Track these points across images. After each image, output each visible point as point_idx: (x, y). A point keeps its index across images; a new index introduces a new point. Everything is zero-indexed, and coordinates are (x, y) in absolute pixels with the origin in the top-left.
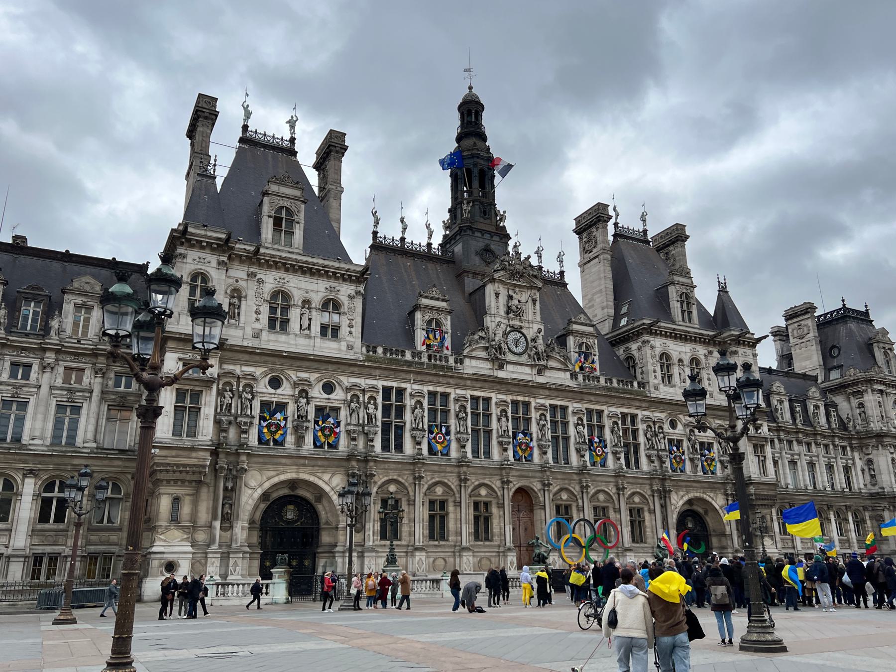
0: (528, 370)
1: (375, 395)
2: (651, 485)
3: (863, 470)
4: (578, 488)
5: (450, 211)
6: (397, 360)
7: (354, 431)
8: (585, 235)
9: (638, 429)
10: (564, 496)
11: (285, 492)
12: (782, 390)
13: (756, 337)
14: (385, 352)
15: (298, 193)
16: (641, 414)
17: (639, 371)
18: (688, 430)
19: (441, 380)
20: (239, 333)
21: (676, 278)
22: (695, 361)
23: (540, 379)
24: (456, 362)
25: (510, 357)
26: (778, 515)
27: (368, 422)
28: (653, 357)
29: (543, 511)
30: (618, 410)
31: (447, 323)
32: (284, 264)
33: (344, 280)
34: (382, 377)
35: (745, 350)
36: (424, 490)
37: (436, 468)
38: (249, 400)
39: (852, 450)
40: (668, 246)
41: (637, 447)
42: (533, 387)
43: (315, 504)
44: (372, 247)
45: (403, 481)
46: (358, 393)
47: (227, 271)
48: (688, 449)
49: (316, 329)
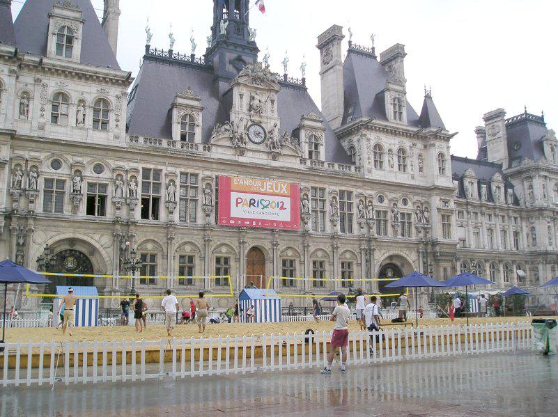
0: (265, 156)
1: (135, 174)
2: (360, 245)
3: (528, 235)
4: (301, 247)
5: (212, 28)
7: (119, 203)
8: (324, 50)
9: (352, 203)
10: (290, 253)
11: (66, 247)
12: (473, 174)
13: (450, 133)
14: (146, 142)
15: (77, 15)
16: (356, 191)
17: (357, 158)
18: (392, 204)
19: (191, 163)
20: (27, 126)
21: (391, 86)
22: (401, 151)
23: (275, 164)
24: (204, 150)
26: (461, 267)
27: (130, 195)
28: (368, 147)
29: (271, 265)
30: (337, 189)
32: (64, 72)
33: (113, 84)
34: (141, 161)
35: (441, 144)
36: (175, 248)
37: (185, 231)
38: (35, 178)
39: (521, 219)
40: (391, 61)
41: (351, 216)
42: (268, 169)
43: (89, 257)
44: (145, 57)
45: (159, 241)
47: (17, 77)
48: (391, 218)
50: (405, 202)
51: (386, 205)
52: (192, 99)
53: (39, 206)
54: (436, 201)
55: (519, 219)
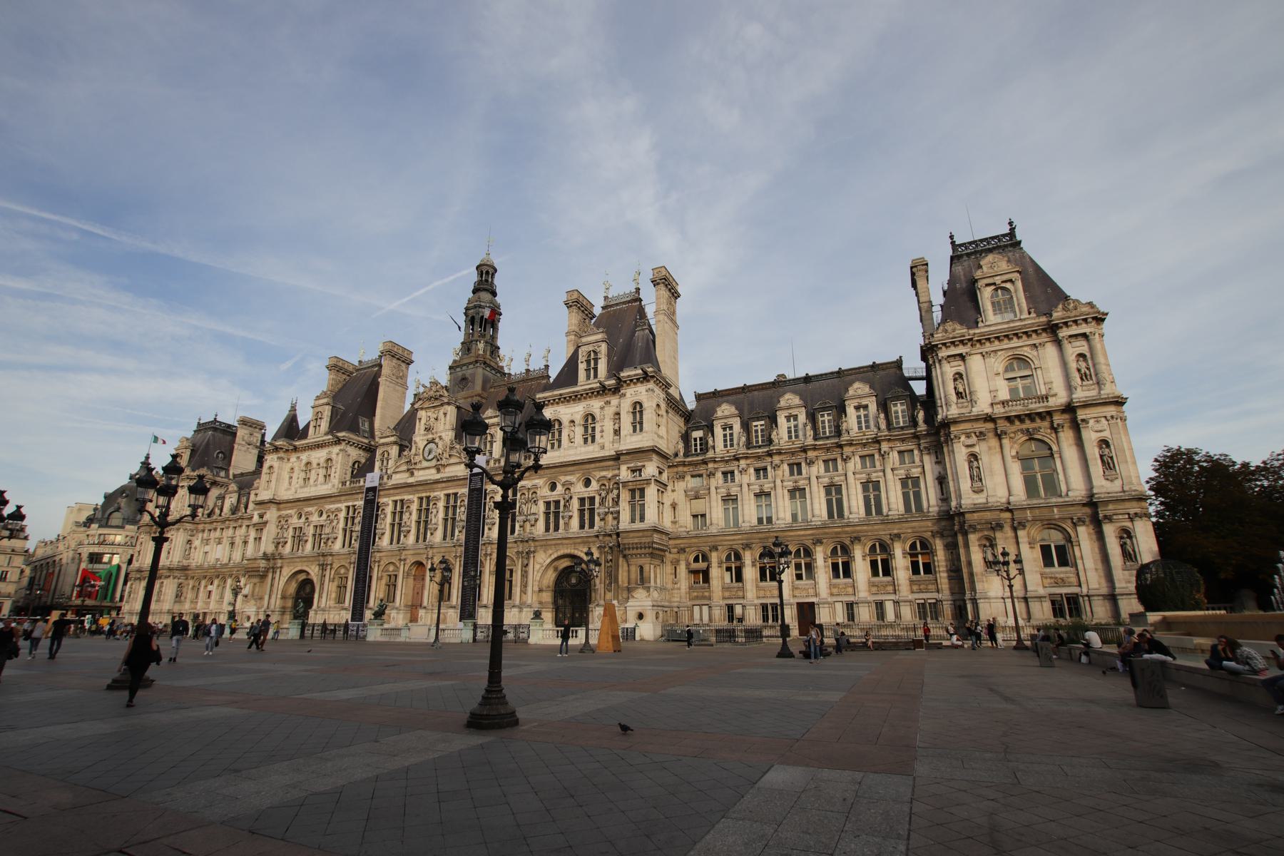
0: (433, 471)
6: (355, 487)
11: (302, 577)
12: (796, 400)
14: (350, 484)
21: (584, 340)
22: (590, 418)
23: (438, 476)
24: (388, 479)
25: (425, 464)
31: (394, 450)
34: (346, 501)
35: (637, 389)
39: (920, 451)
46: (330, 514)
49: (321, 479)
50: (587, 483)
51: (558, 493)
52: (388, 437)
53: (287, 549)
54: (624, 474)
55: (916, 452)
